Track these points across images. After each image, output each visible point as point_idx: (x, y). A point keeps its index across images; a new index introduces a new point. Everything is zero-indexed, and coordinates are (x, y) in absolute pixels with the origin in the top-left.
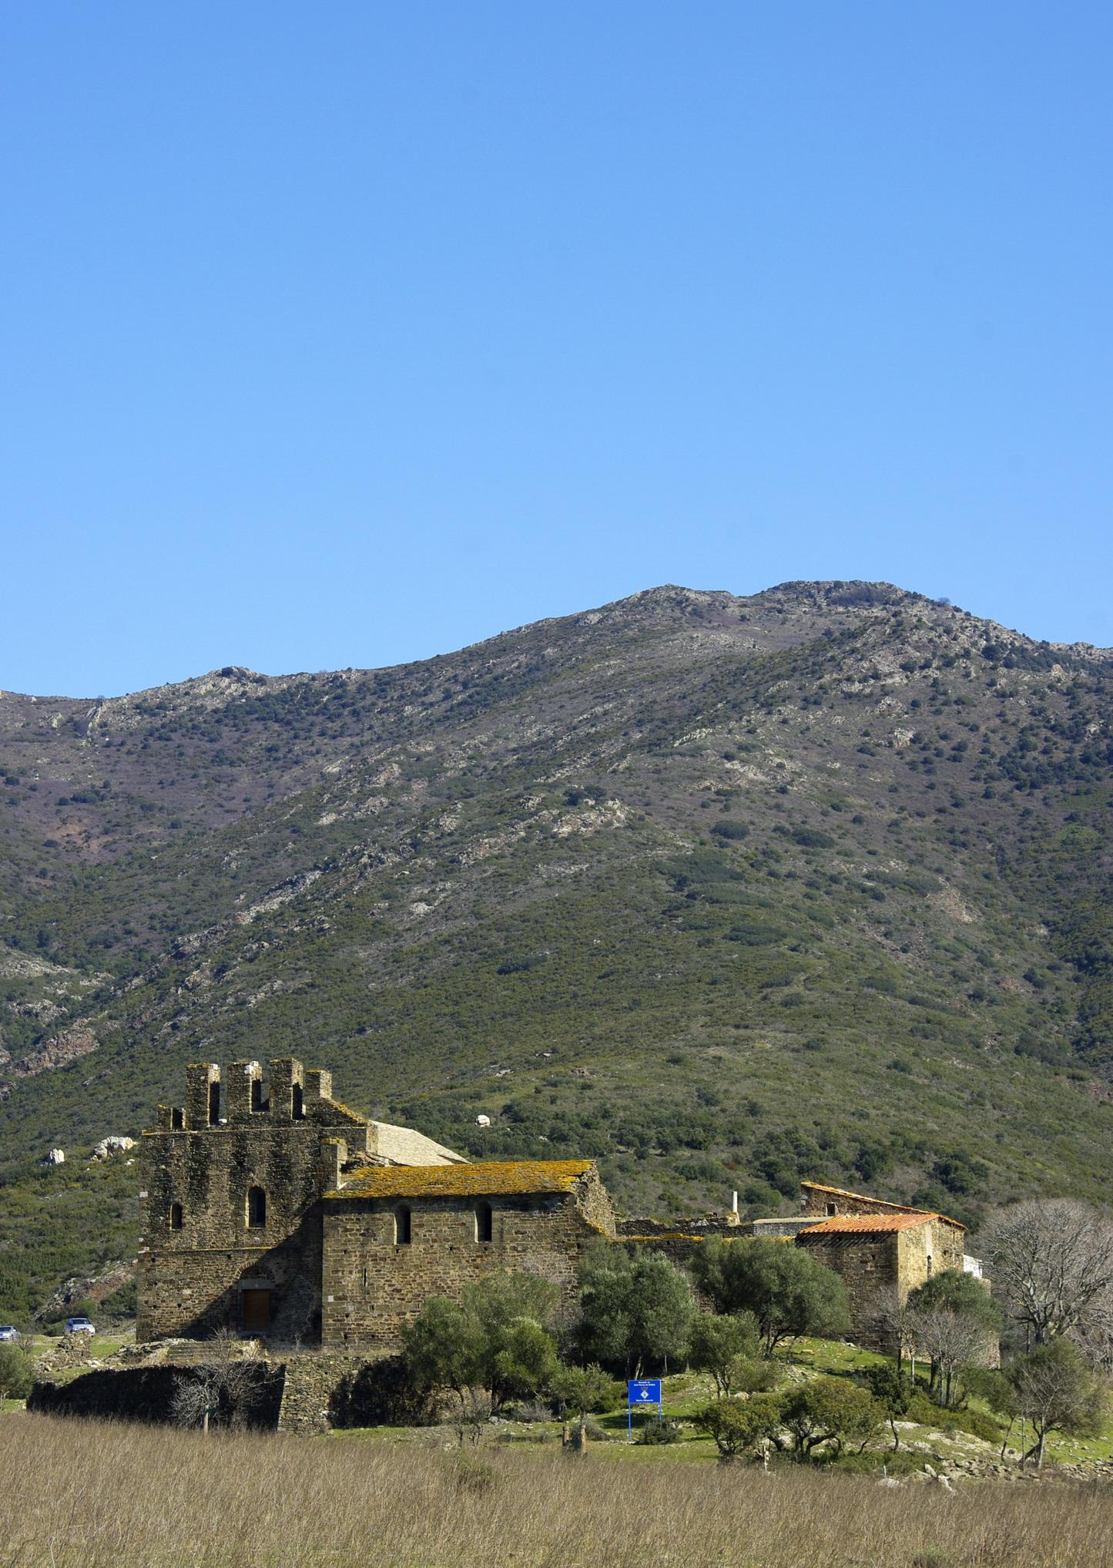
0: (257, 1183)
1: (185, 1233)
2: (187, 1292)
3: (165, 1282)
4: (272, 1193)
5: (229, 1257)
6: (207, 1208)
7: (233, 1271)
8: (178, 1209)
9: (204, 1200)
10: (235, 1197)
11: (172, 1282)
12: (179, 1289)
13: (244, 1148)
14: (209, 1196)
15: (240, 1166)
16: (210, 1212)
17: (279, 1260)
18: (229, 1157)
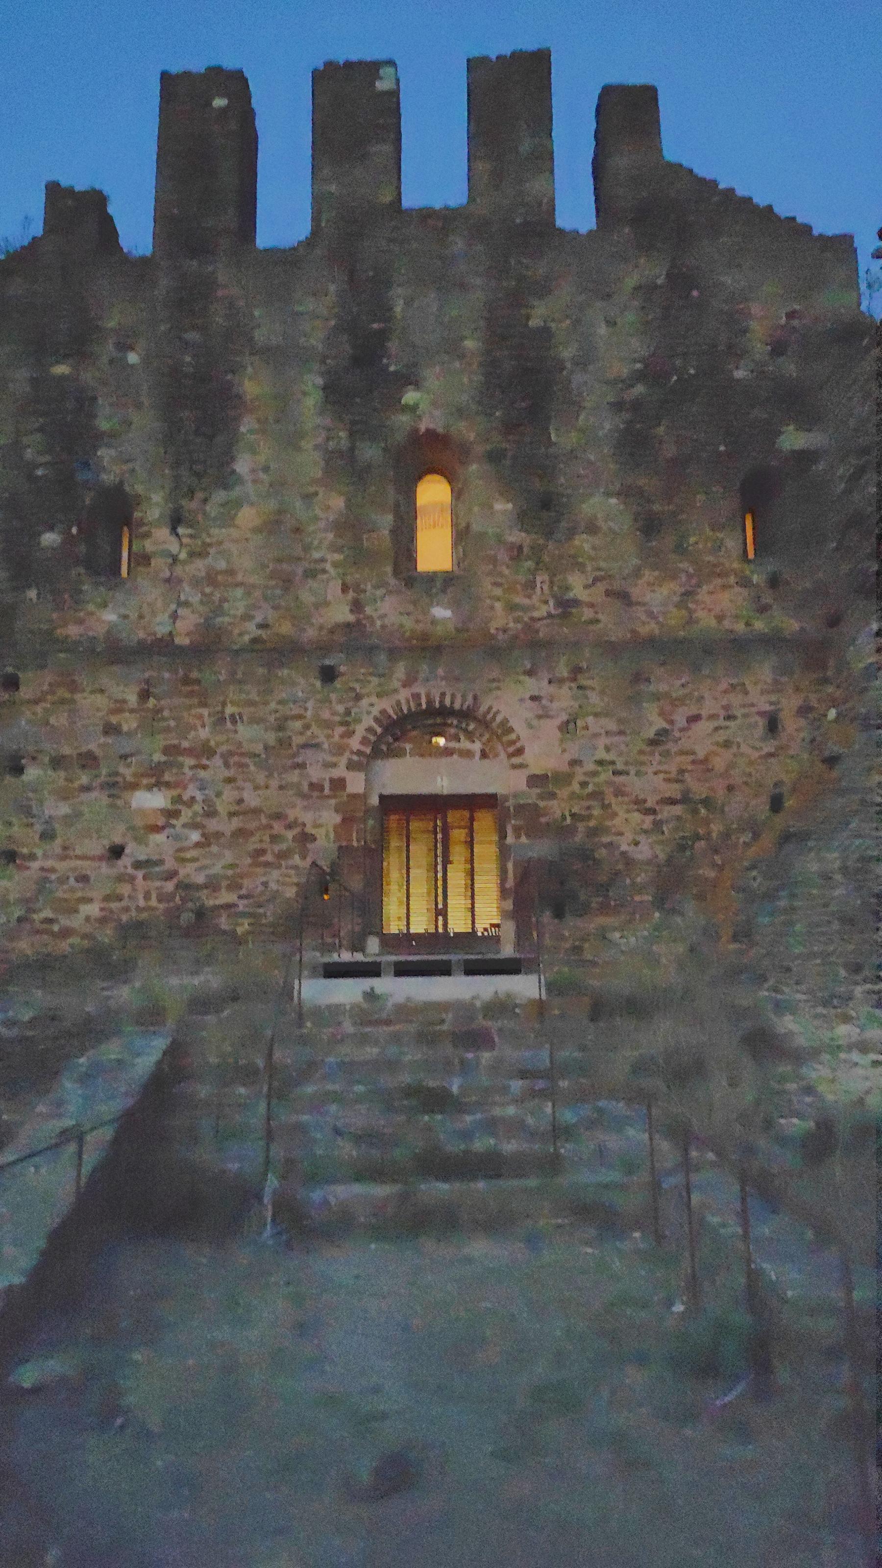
0: (431, 420)
1: (150, 592)
2: (150, 801)
3: (57, 762)
4: (494, 457)
5: (328, 675)
6: (238, 504)
7: (347, 722)
8: (117, 511)
9: (226, 478)
10: (344, 467)
11: (88, 760)
12: (115, 787)
13: (384, 311)
14: (242, 466)
15: (364, 375)
16: (247, 516)
17: (532, 686)
18: (315, 337)
